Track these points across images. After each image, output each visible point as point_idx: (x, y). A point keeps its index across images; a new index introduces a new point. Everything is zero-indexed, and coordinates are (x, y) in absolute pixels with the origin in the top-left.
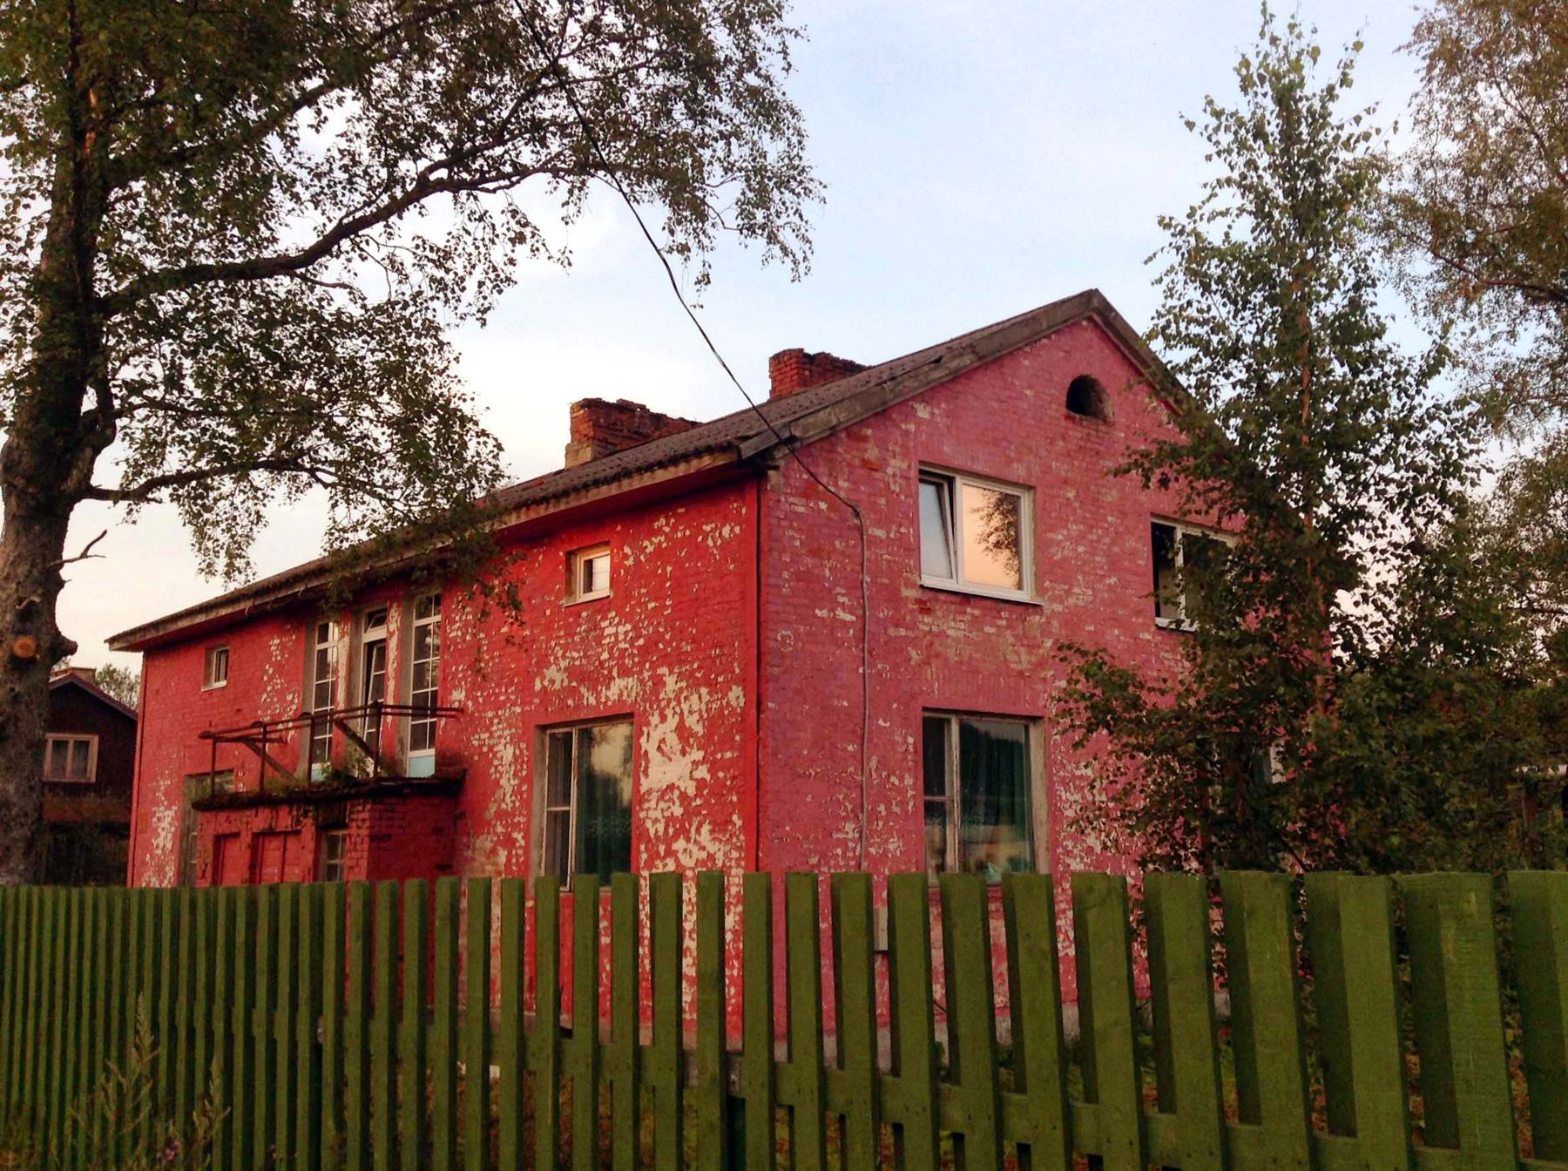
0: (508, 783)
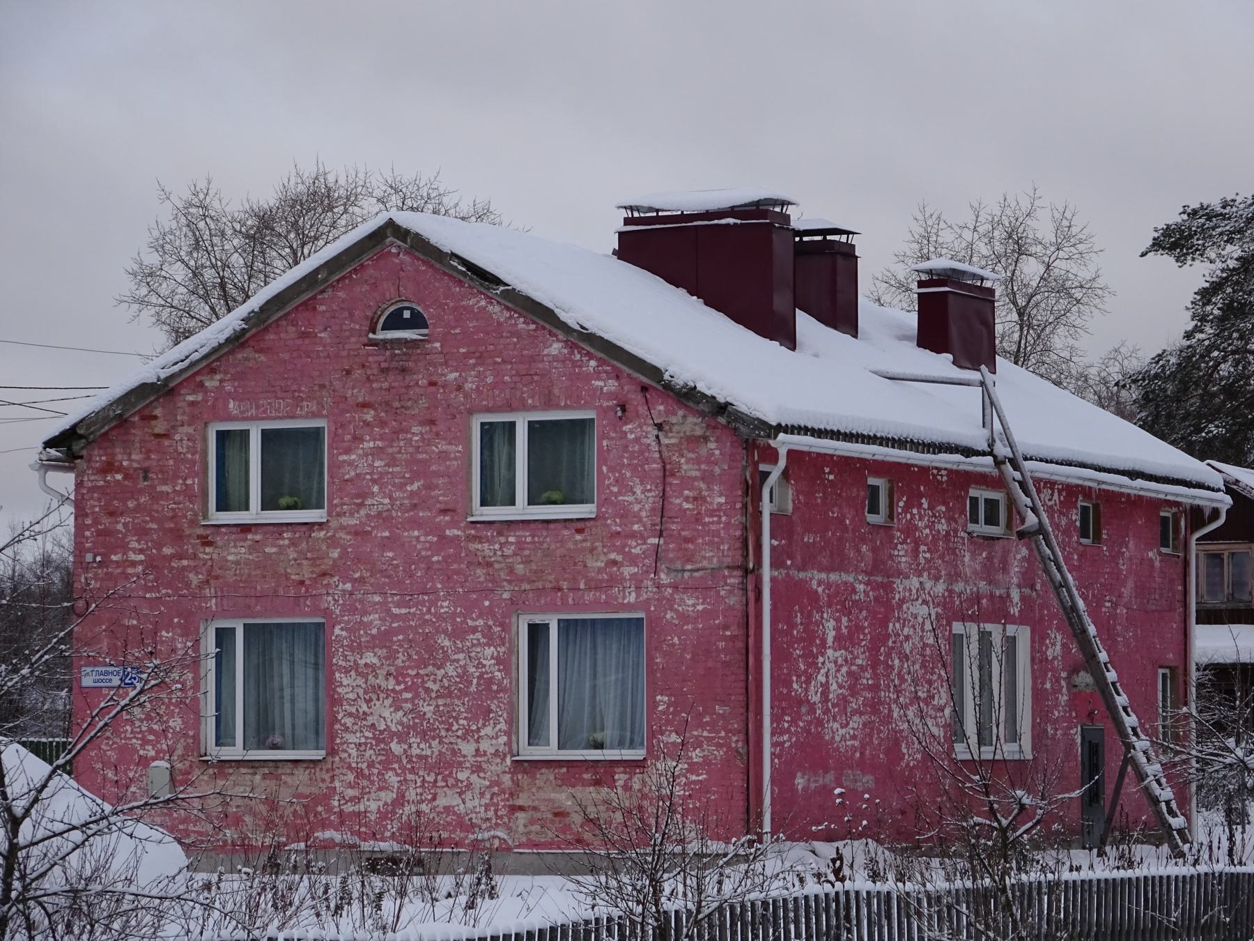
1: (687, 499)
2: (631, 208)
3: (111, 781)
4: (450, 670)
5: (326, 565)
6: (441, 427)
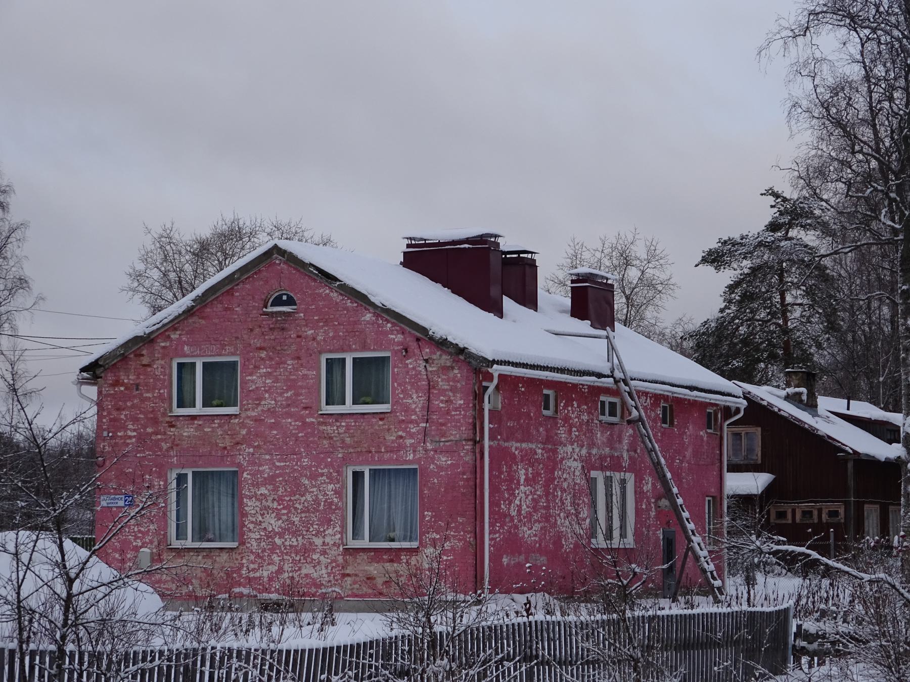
1: (442, 401)
2: (411, 239)
3: (117, 560)
4: (309, 497)
5: (239, 438)
6: (304, 361)
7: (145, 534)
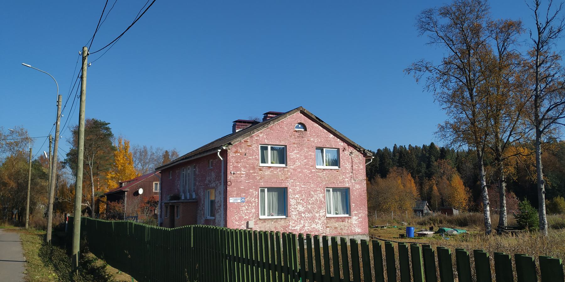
0: (202, 199)
4: (314, 198)
7: (250, 213)
